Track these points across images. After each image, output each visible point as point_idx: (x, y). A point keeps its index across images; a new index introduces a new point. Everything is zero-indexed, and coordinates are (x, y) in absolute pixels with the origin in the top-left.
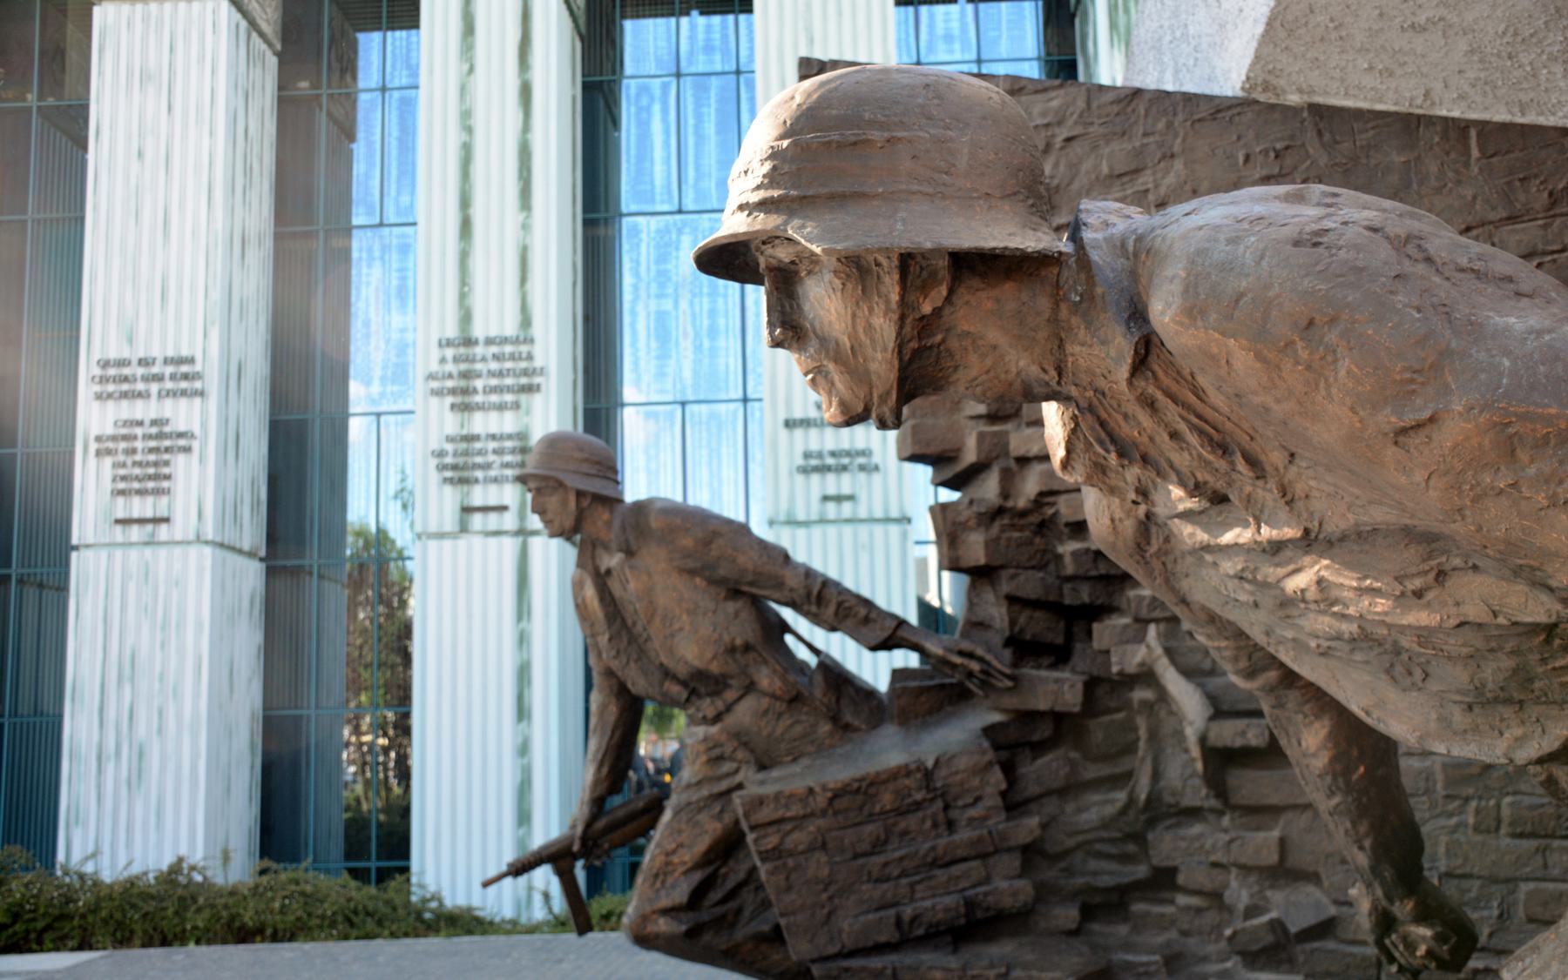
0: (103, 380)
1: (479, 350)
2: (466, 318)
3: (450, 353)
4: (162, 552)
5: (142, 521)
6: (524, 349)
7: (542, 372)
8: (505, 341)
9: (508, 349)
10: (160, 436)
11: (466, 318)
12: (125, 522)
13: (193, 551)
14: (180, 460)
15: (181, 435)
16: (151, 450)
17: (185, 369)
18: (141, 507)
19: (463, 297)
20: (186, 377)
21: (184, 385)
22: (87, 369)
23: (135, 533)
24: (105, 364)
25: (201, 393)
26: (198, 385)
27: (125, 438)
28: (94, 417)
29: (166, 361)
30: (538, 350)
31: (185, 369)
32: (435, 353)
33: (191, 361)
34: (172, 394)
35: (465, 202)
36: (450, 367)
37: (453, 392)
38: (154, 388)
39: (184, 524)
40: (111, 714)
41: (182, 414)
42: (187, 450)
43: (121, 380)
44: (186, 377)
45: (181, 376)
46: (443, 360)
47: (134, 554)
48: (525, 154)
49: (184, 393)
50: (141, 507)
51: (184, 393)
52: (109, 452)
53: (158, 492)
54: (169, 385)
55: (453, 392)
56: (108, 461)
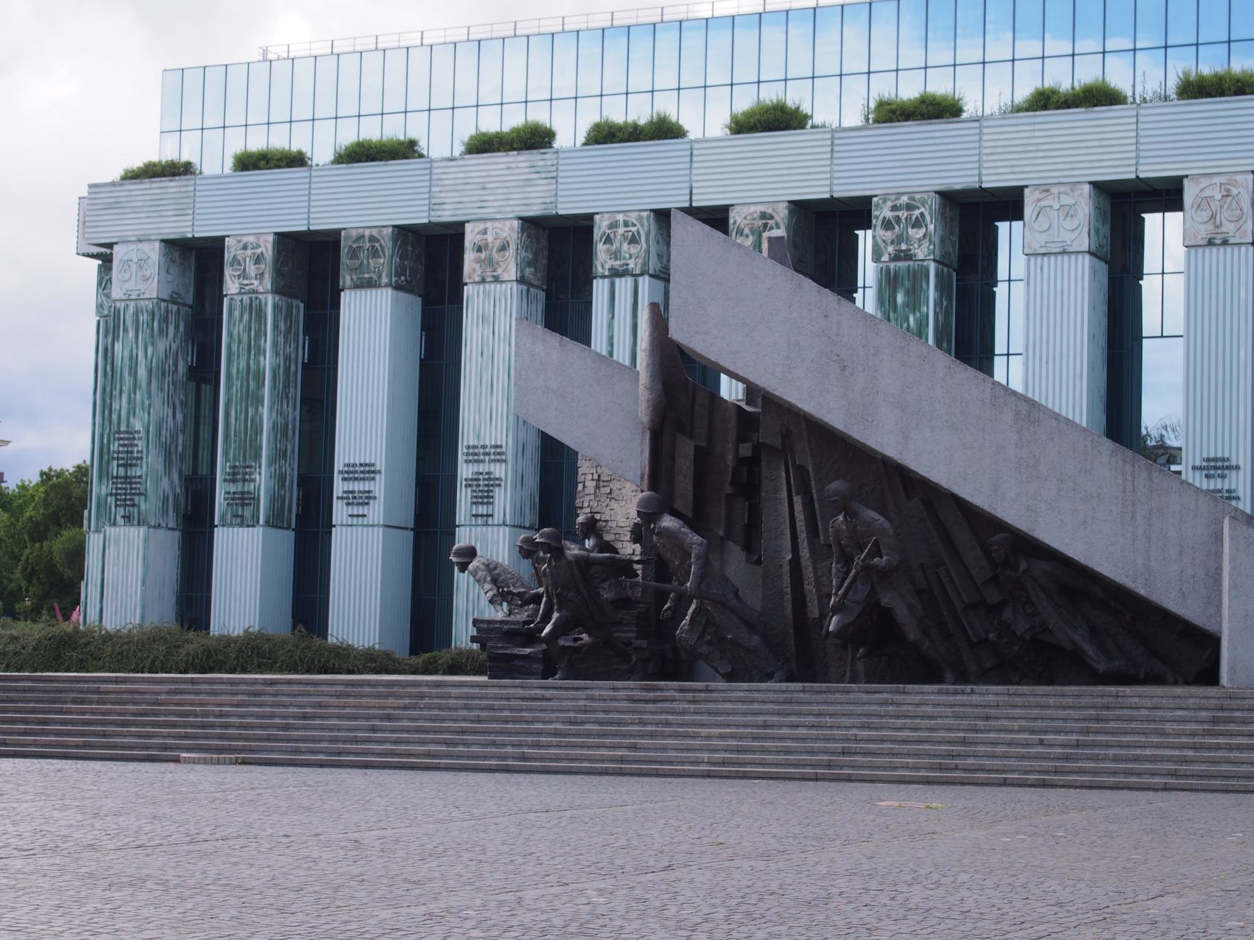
0: (468, 454)
4: (490, 529)
5: (482, 516)
10: (489, 479)
12: (476, 516)
13: (501, 529)
14: (497, 489)
16: (487, 485)
18: (482, 510)
20: (499, 454)
22: (462, 450)
23: (480, 521)
24: (468, 447)
25: (505, 461)
27: (477, 480)
28: (465, 471)
34: (494, 461)
38: (487, 458)
39: (498, 518)
40: (471, 596)
41: (498, 470)
42: (499, 485)
43: (475, 456)
44: (499, 454)
45: (497, 453)
47: (479, 529)
50: (482, 510)
52: (470, 486)
53: (488, 503)
56: (469, 490)
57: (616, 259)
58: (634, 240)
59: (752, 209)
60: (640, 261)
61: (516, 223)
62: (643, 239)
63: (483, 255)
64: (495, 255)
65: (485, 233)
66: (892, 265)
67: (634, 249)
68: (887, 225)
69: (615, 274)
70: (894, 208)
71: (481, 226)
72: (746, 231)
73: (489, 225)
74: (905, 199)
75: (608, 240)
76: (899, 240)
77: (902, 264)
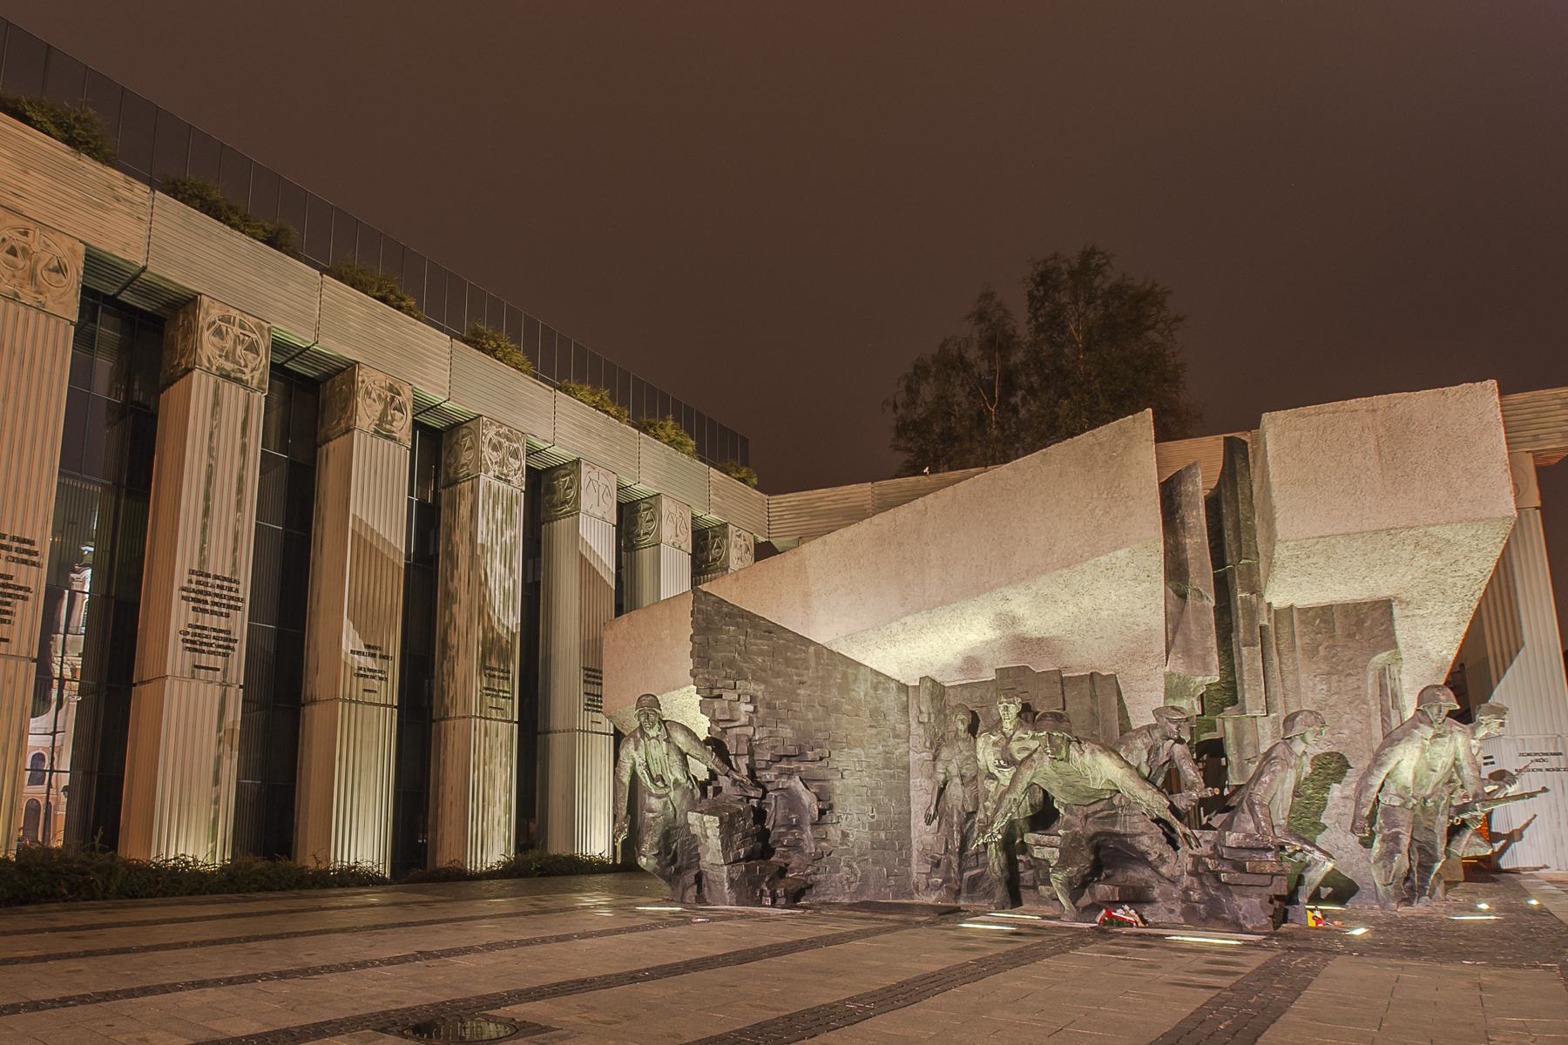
1: (210, 580)
2: (203, 562)
3: (194, 578)
6: (234, 585)
7: (243, 600)
8: (225, 579)
9: (226, 584)
11: (203, 562)
15: (20, 588)
17: (26, 546)
19: (202, 549)
21: (25, 557)
26: (35, 559)
29: (13, 539)
30: (241, 588)
31: (26, 546)
32: (187, 577)
33: (32, 543)
34: (14, 560)
35: (207, 498)
36: (193, 586)
37: (194, 600)
42: (25, 598)
46: (190, 581)
48: (240, 479)
49: (25, 562)
51: (25, 562)
54: (14, 554)
55: (194, 600)
57: (227, 358)
58: (253, 348)
59: (382, 376)
60: (257, 374)
61: (81, 249)
62: (262, 352)
63: (20, 262)
64: (43, 275)
65: (26, 234)
66: (496, 483)
67: (250, 356)
68: (495, 448)
69: (227, 377)
70: (498, 434)
71: (18, 222)
72: (374, 395)
73: (31, 225)
74: (504, 430)
75: (219, 333)
76: (502, 463)
77: (502, 485)
